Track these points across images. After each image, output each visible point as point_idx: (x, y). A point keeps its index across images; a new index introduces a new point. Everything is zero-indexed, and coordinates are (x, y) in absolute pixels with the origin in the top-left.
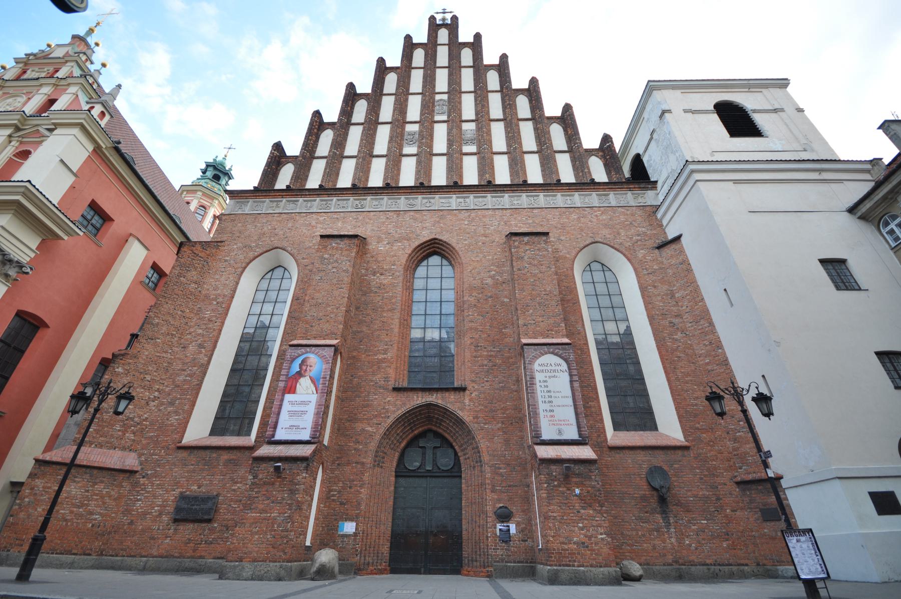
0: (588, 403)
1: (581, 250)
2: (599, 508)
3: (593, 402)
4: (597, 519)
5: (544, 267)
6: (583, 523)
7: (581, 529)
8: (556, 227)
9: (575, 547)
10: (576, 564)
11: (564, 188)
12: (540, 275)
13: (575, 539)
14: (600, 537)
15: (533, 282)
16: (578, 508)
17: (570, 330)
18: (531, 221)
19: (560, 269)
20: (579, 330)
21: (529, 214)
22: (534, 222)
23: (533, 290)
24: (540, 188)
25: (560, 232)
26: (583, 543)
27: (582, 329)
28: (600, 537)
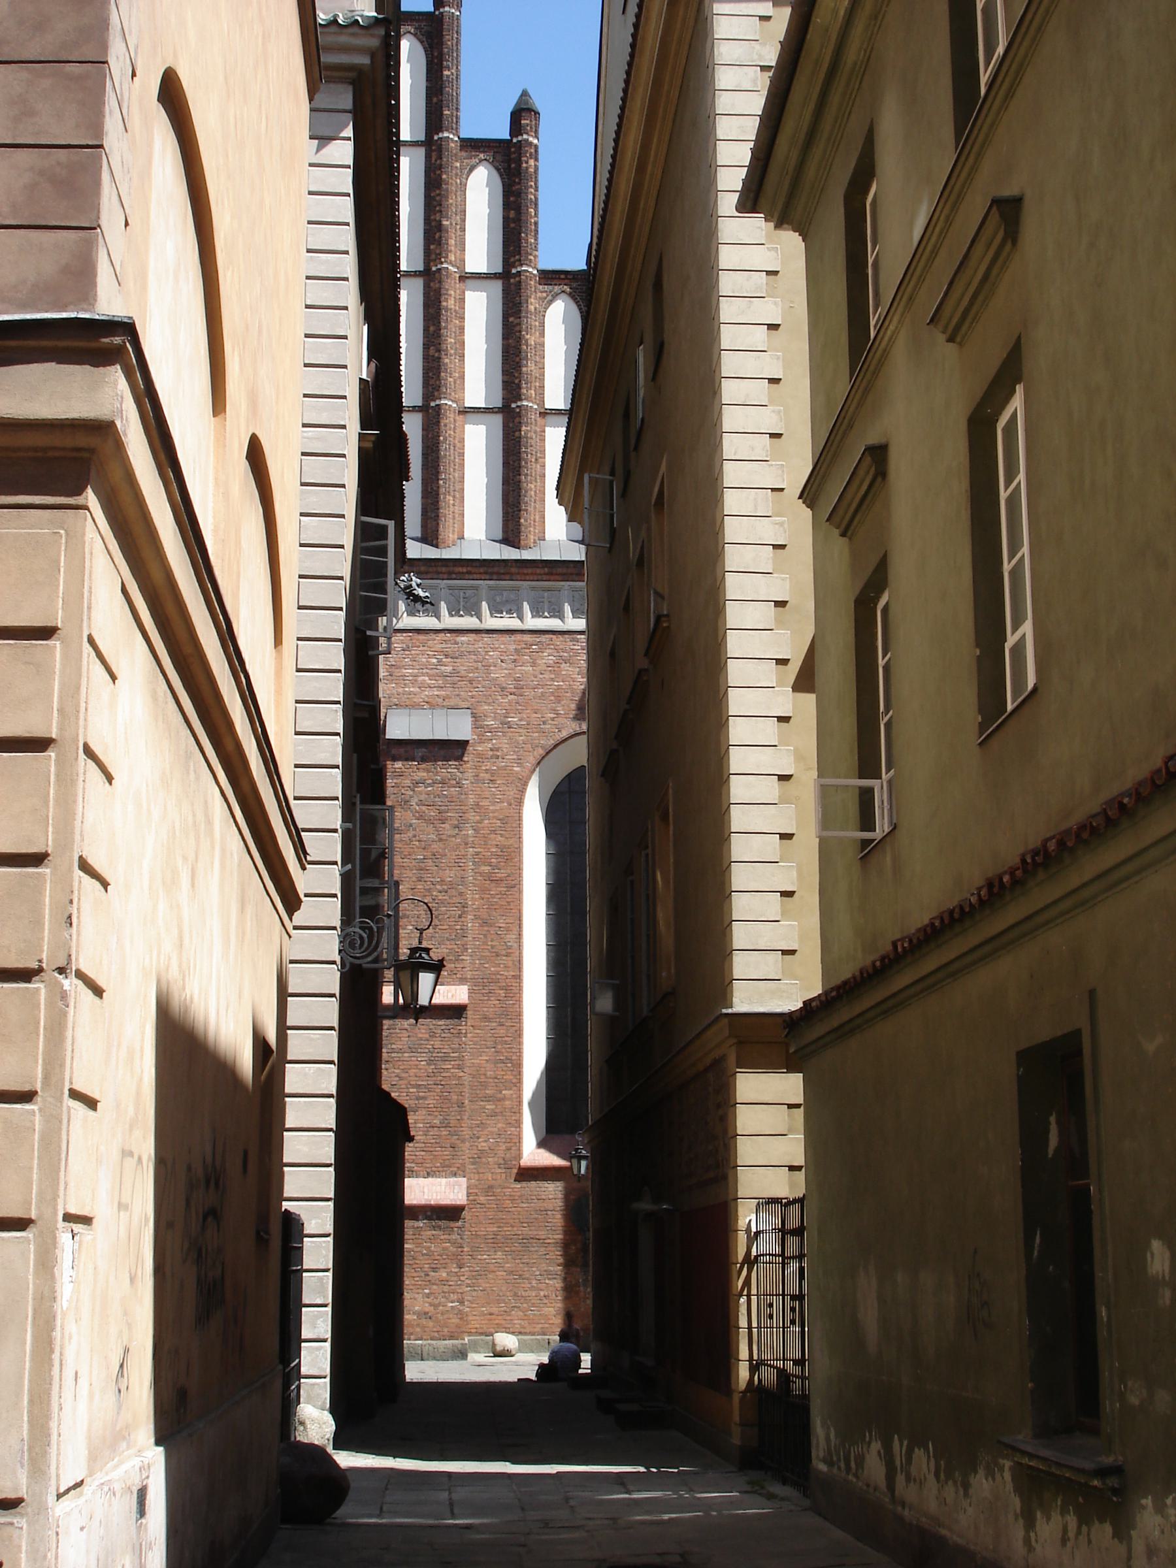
0: (501, 1092)
1: (547, 753)
2: (456, 1270)
3: (511, 1089)
4: (451, 1283)
5: (446, 826)
6: (430, 1289)
7: (428, 1296)
8: (503, 689)
9: (415, 1317)
10: (412, 1337)
11: (538, 571)
12: (436, 847)
13: (417, 1308)
14: (451, 1305)
15: (422, 861)
16: (426, 1270)
17: (493, 947)
18: (449, 669)
19: (494, 803)
20: (510, 947)
21: (450, 648)
22: (455, 672)
23: (420, 880)
24: (482, 570)
25: (510, 702)
26: (426, 1313)
27: (516, 945)
28: (451, 1305)
